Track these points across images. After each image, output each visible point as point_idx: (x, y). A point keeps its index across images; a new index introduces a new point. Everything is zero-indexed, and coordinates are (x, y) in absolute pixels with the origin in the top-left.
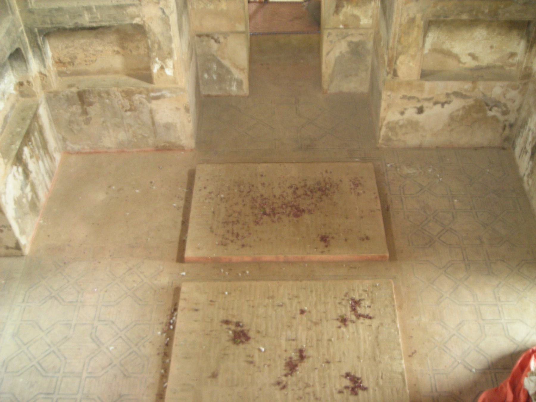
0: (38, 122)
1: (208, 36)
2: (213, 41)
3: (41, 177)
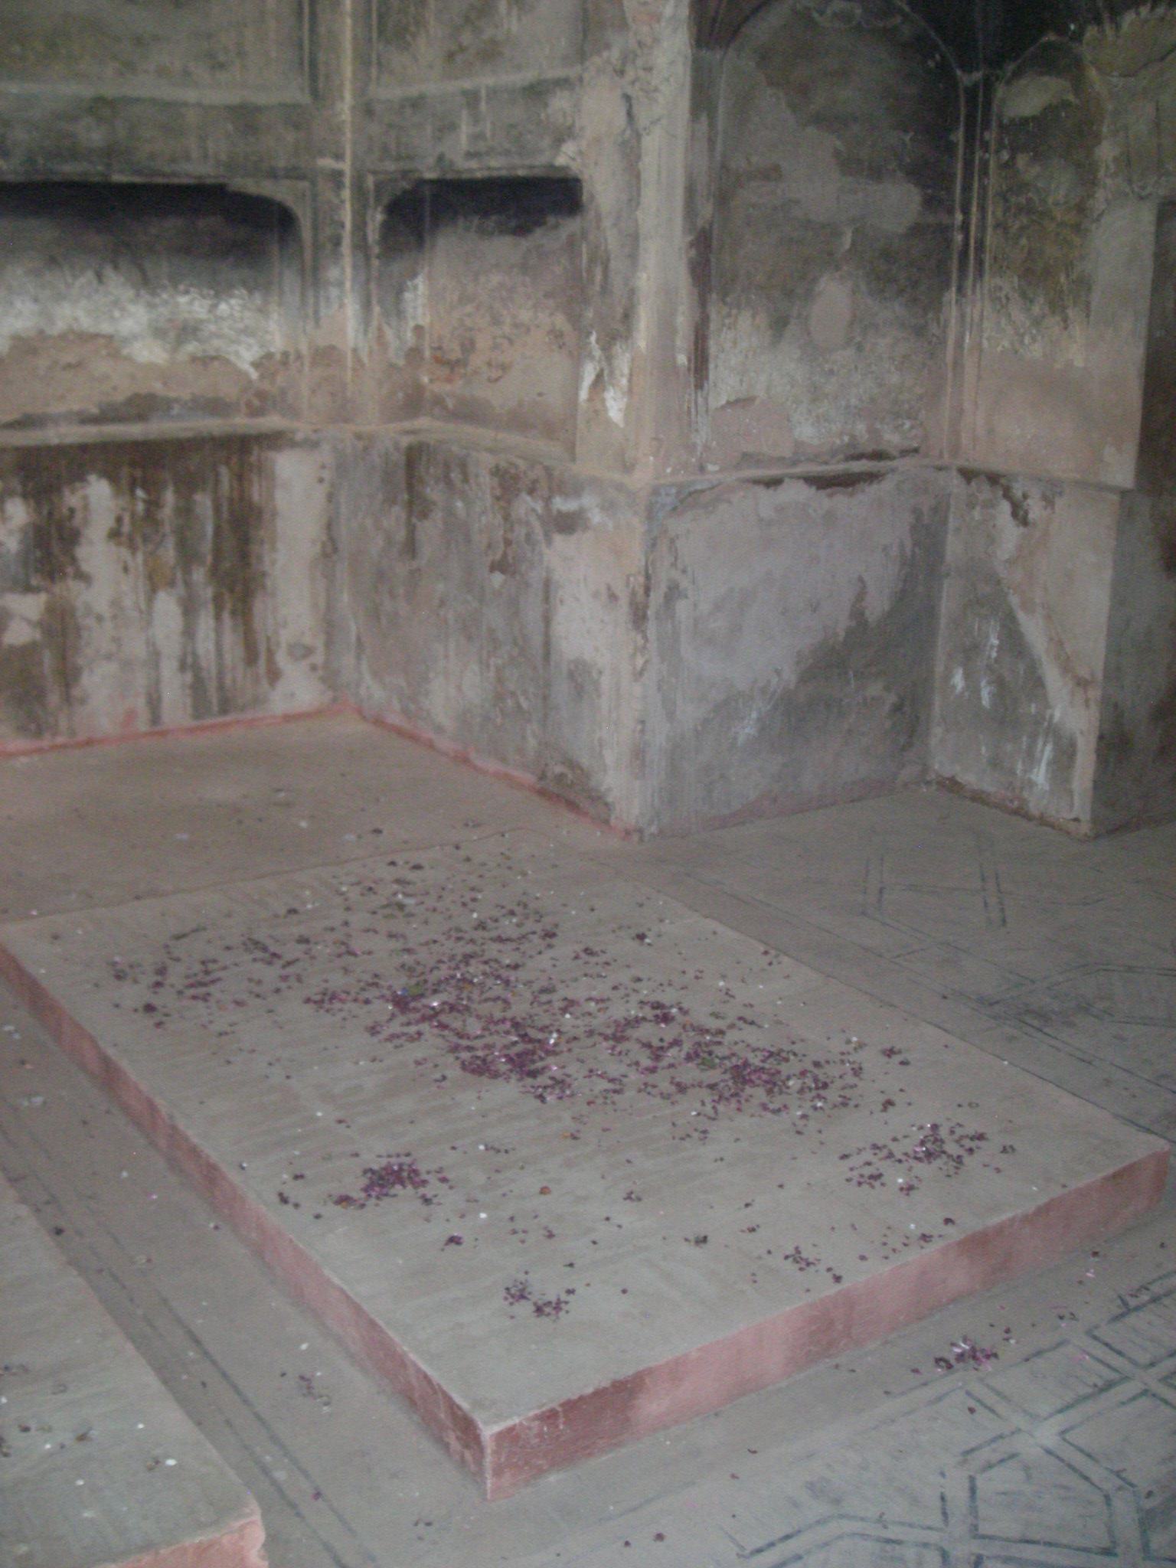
0: (240, 477)
1: (993, 479)
2: (1005, 507)
3: (137, 648)
